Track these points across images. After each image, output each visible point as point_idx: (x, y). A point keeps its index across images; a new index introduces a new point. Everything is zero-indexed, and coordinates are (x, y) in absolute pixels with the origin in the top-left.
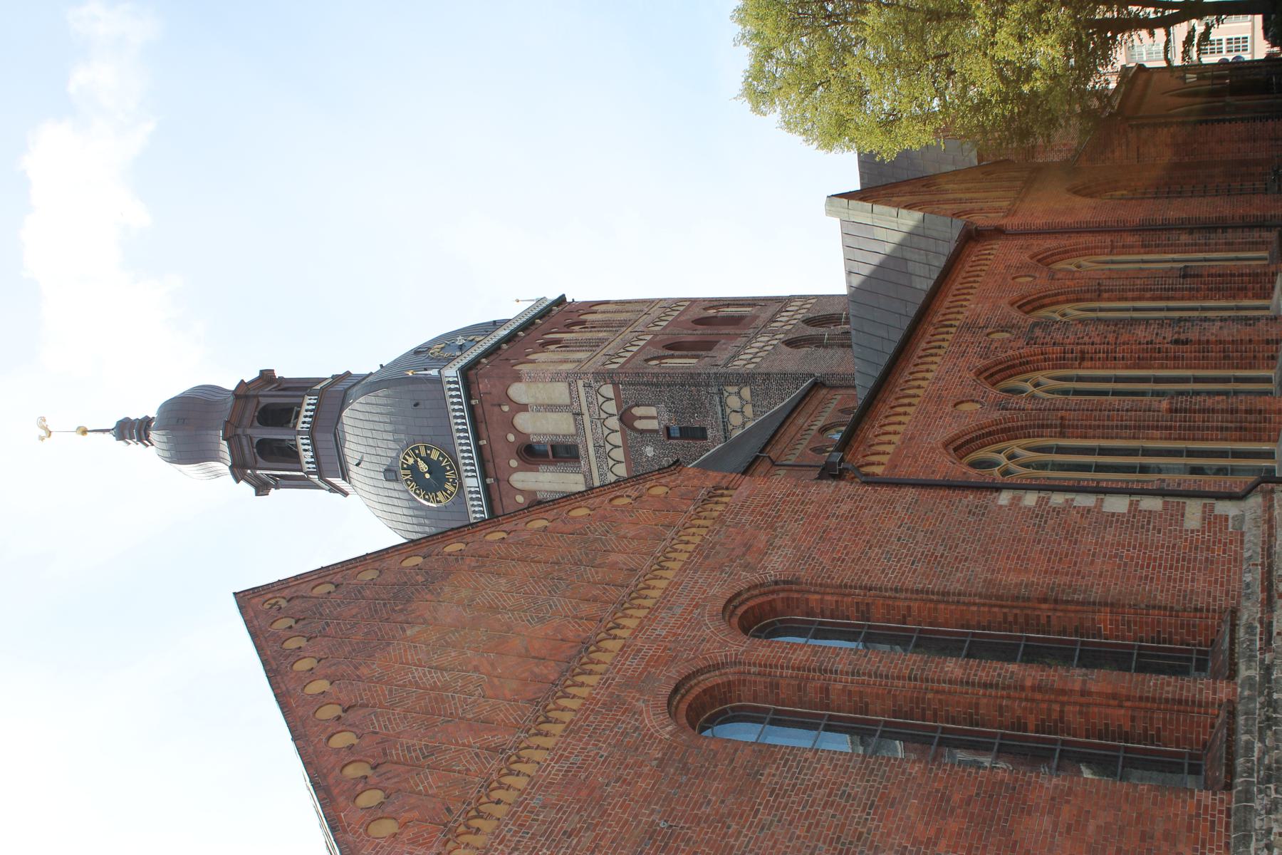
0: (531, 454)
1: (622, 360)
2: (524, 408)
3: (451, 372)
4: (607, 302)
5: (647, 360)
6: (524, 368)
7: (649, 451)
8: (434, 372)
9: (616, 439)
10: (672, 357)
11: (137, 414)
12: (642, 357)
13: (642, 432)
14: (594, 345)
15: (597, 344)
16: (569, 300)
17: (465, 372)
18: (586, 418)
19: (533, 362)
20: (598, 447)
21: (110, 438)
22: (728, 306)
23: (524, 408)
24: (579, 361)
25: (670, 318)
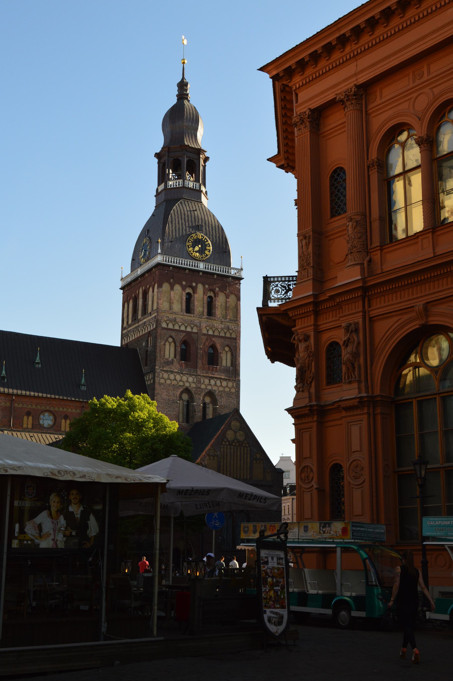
0: (145, 294)
1: (170, 326)
2: (153, 291)
3: (159, 259)
4: (239, 299)
5: (171, 337)
6: (166, 286)
7: (144, 344)
8: (159, 251)
9: (146, 331)
10: (175, 346)
11: (190, 90)
12: (173, 334)
13: (148, 340)
14: (189, 309)
15: (189, 309)
16: (241, 281)
17: (158, 265)
18: (150, 317)
19: (172, 289)
20: (145, 323)
21: (180, 80)
22: (232, 355)
23: (153, 291)
24: (171, 308)
25: (216, 333)
